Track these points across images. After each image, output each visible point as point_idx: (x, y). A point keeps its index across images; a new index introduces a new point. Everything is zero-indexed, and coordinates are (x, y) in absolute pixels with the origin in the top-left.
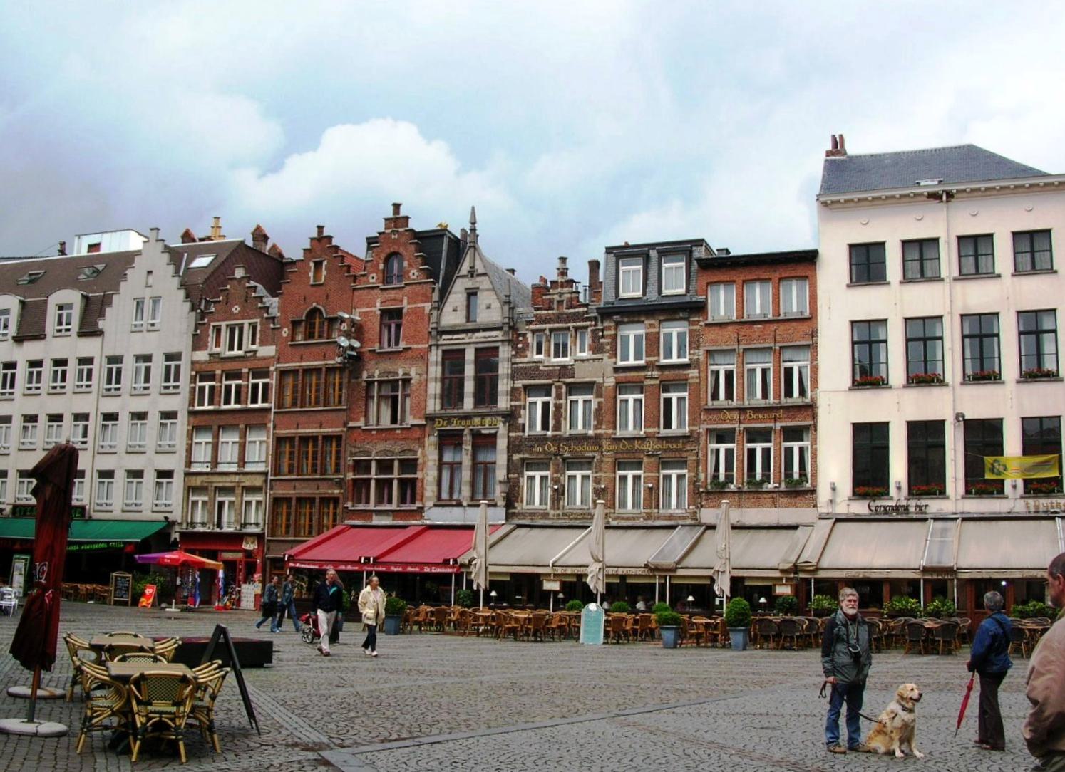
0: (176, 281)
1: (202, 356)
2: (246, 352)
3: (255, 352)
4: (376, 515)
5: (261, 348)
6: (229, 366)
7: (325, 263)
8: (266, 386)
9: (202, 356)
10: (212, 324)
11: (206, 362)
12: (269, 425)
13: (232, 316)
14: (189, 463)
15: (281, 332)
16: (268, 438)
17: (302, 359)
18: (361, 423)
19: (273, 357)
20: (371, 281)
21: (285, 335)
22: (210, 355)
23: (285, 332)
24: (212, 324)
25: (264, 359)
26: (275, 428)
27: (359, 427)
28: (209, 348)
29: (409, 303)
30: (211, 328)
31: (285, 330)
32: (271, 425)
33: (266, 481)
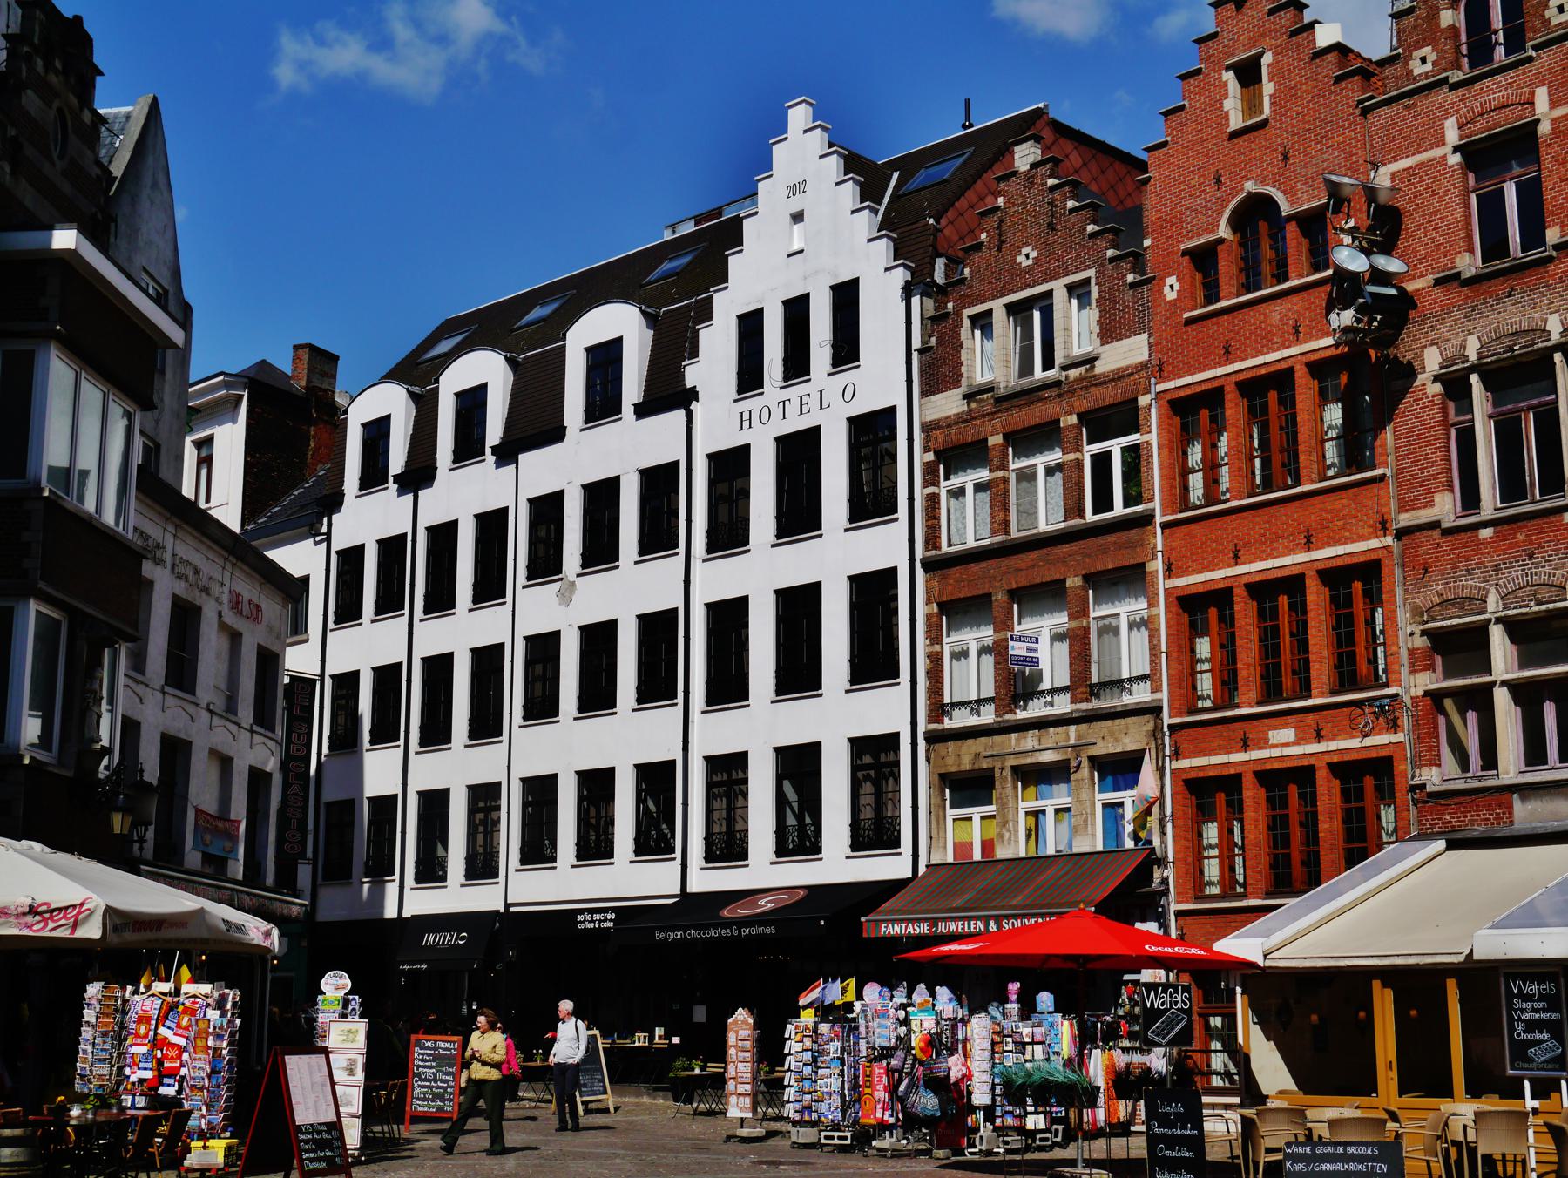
0: (865, 222)
1: (949, 404)
2: (1064, 368)
3: (1090, 360)
4: (1523, 799)
5: (1107, 347)
6: (1022, 417)
7: (1267, 59)
8: (1134, 456)
9: (949, 404)
10: (967, 312)
11: (961, 420)
12: (1150, 567)
13: (1024, 278)
14: (939, 710)
15: (1161, 292)
16: (1152, 604)
17: (1228, 355)
18: (1445, 508)
19: (1144, 366)
20: (1418, 69)
21: (1171, 296)
22: (968, 397)
23: (1171, 288)
24: (967, 312)
25: (1119, 376)
26: (1170, 571)
27: (1435, 525)
28: (964, 382)
29: (1554, 104)
30: (966, 323)
31: (1172, 280)
32: (1157, 565)
33: (1156, 733)
